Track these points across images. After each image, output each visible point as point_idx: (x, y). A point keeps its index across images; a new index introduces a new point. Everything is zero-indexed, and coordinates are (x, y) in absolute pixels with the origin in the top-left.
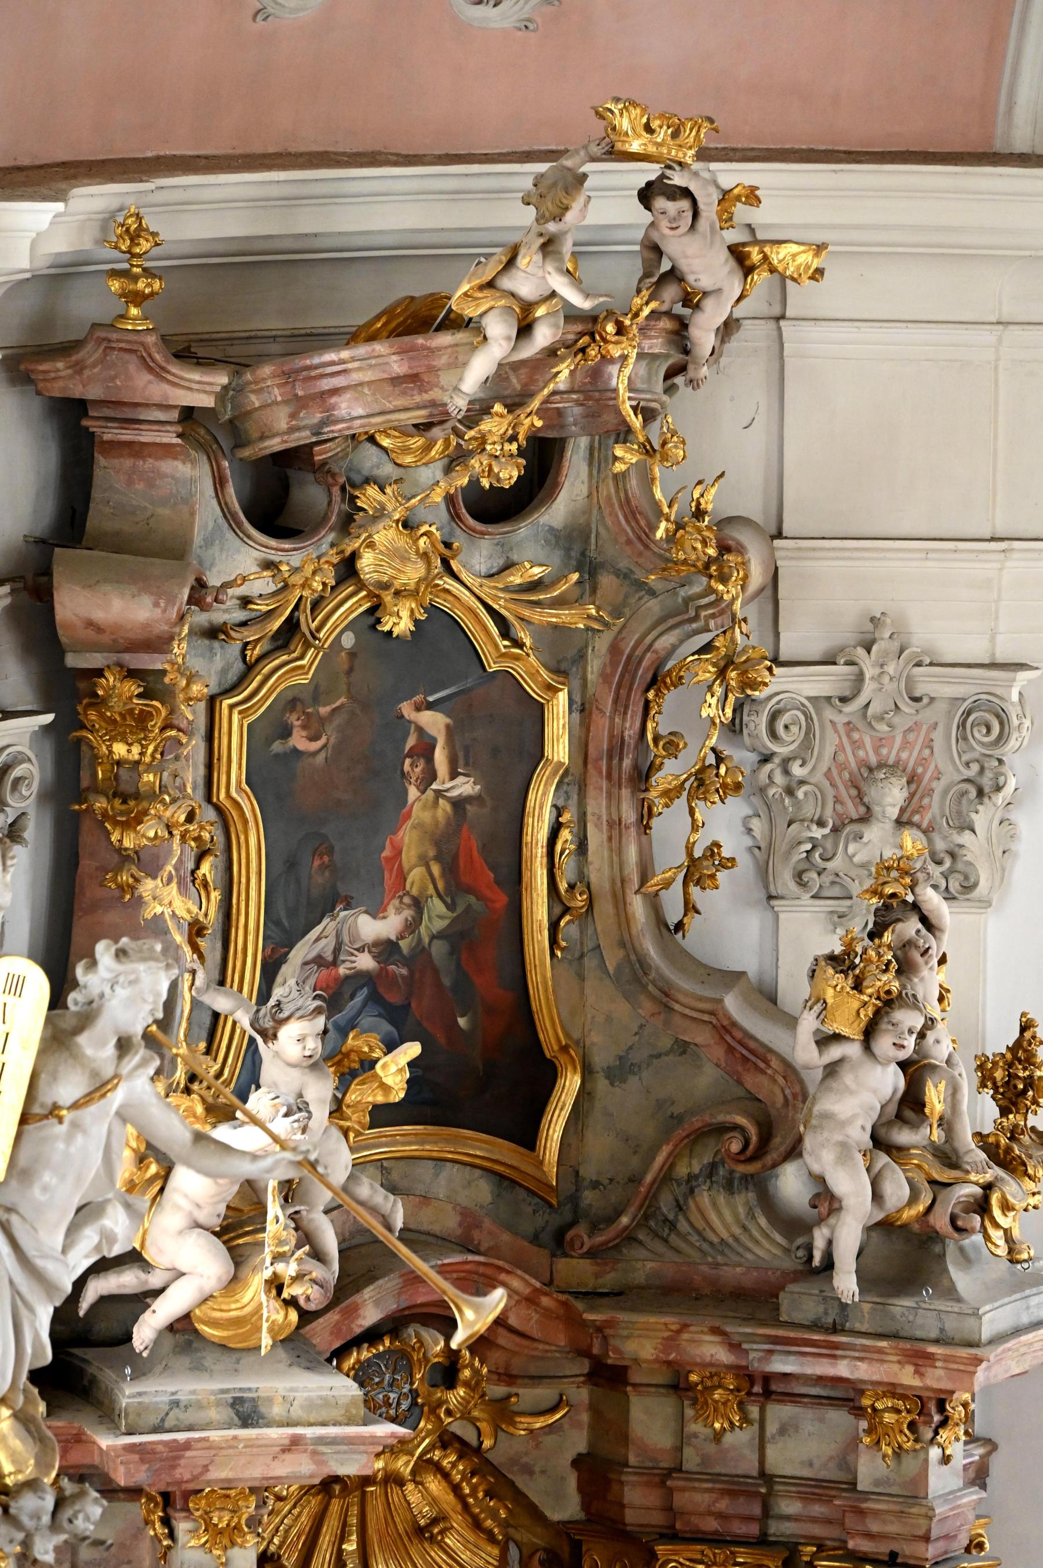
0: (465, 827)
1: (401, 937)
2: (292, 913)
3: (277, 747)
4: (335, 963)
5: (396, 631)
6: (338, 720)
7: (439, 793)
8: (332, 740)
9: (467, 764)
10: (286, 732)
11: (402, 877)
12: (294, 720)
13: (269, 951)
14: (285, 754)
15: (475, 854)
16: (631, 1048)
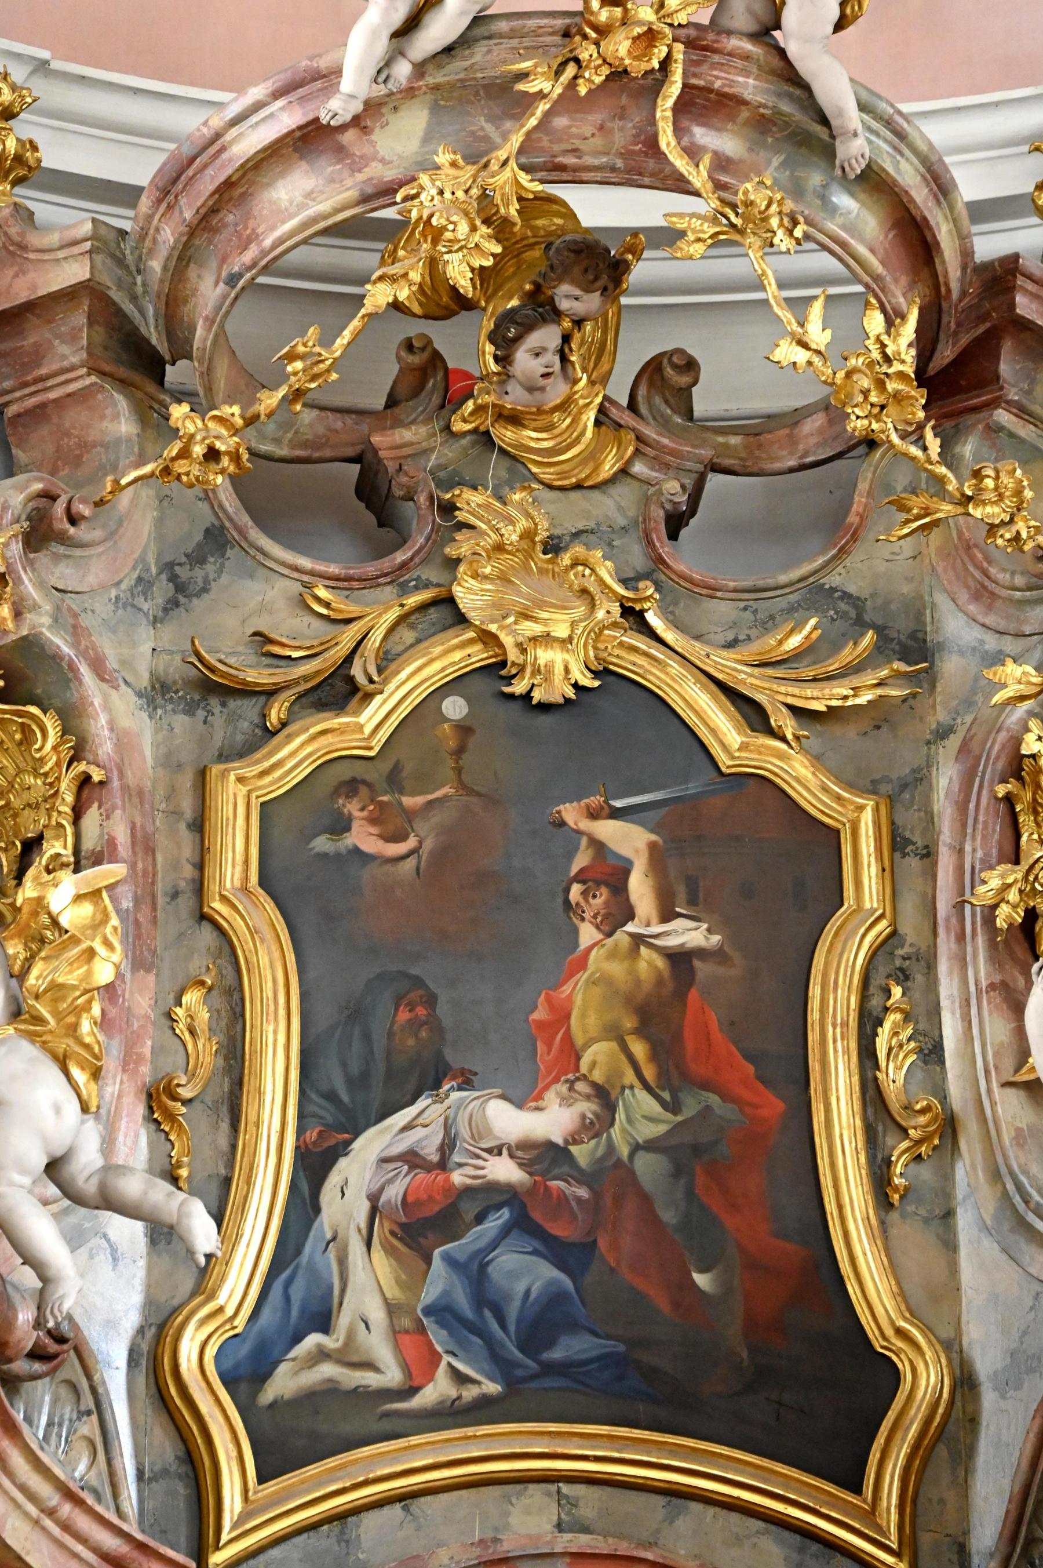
0: (693, 995)
1: (574, 1139)
2: (359, 1082)
3: (322, 844)
4: (443, 1165)
5: (537, 696)
6: (437, 818)
7: (638, 940)
8: (428, 845)
9: (692, 901)
10: (341, 826)
11: (572, 1054)
12: (352, 807)
13: (311, 1135)
14: (338, 856)
15: (717, 1035)
16: (1025, 1333)
